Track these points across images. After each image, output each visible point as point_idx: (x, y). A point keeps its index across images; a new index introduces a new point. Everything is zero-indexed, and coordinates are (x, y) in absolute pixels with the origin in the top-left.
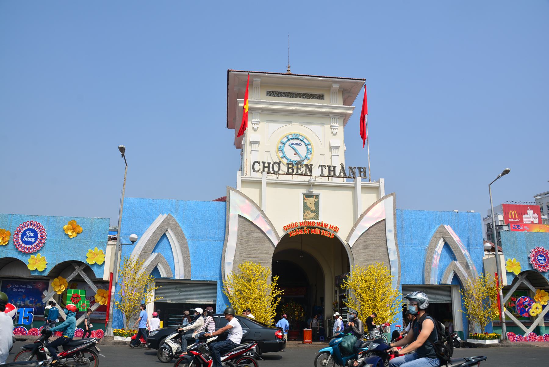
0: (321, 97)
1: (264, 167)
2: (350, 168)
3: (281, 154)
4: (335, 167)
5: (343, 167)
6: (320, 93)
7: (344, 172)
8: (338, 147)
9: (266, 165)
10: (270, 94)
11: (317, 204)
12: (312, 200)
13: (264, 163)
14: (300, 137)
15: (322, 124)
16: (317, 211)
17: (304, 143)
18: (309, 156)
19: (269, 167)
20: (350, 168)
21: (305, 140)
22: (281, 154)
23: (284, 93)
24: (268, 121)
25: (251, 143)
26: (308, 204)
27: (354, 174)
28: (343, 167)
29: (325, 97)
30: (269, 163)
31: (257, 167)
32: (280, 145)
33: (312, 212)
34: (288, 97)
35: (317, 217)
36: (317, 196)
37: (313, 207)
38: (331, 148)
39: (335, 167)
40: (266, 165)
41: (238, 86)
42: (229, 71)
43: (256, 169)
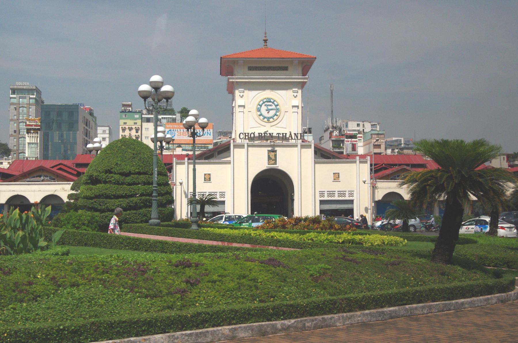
0: (286, 69)
1: (245, 136)
2: (295, 134)
3: (259, 113)
4: (286, 134)
5: (291, 134)
6: (286, 65)
7: (291, 137)
8: (298, 107)
9: (247, 135)
10: (250, 69)
11: (275, 156)
12: (273, 154)
13: (245, 134)
14: (272, 100)
15: (287, 89)
16: (275, 160)
17: (274, 104)
18: (278, 114)
19: (248, 136)
20: (295, 134)
21: (275, 102)
22: (259, 113)
23: (260, 67)
24: (249, 90)
25: (239, 106)
26: (271, 156)
27: (297, 137)
28: (291, 134)
29: (289, 68)
30: (248, 134)
31: (242, 136)
32: (259, 106)
33: (273, 160)
34: (262, 70)
35: (275, 163)
36: (276, 151)
37: (273, 158)
38: (293, 106)
39: (286, 134)
40: (247, 135)
41: (228, 67)
42: (221, 58)
43: (241, 137)
